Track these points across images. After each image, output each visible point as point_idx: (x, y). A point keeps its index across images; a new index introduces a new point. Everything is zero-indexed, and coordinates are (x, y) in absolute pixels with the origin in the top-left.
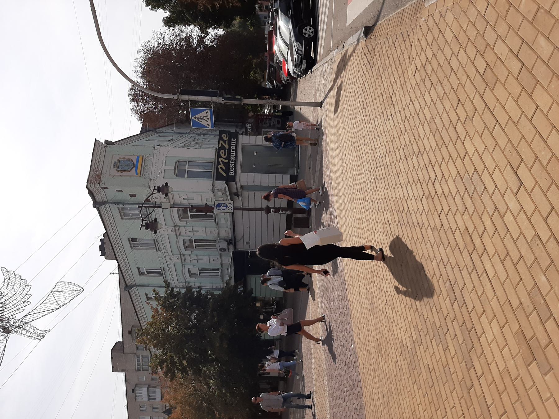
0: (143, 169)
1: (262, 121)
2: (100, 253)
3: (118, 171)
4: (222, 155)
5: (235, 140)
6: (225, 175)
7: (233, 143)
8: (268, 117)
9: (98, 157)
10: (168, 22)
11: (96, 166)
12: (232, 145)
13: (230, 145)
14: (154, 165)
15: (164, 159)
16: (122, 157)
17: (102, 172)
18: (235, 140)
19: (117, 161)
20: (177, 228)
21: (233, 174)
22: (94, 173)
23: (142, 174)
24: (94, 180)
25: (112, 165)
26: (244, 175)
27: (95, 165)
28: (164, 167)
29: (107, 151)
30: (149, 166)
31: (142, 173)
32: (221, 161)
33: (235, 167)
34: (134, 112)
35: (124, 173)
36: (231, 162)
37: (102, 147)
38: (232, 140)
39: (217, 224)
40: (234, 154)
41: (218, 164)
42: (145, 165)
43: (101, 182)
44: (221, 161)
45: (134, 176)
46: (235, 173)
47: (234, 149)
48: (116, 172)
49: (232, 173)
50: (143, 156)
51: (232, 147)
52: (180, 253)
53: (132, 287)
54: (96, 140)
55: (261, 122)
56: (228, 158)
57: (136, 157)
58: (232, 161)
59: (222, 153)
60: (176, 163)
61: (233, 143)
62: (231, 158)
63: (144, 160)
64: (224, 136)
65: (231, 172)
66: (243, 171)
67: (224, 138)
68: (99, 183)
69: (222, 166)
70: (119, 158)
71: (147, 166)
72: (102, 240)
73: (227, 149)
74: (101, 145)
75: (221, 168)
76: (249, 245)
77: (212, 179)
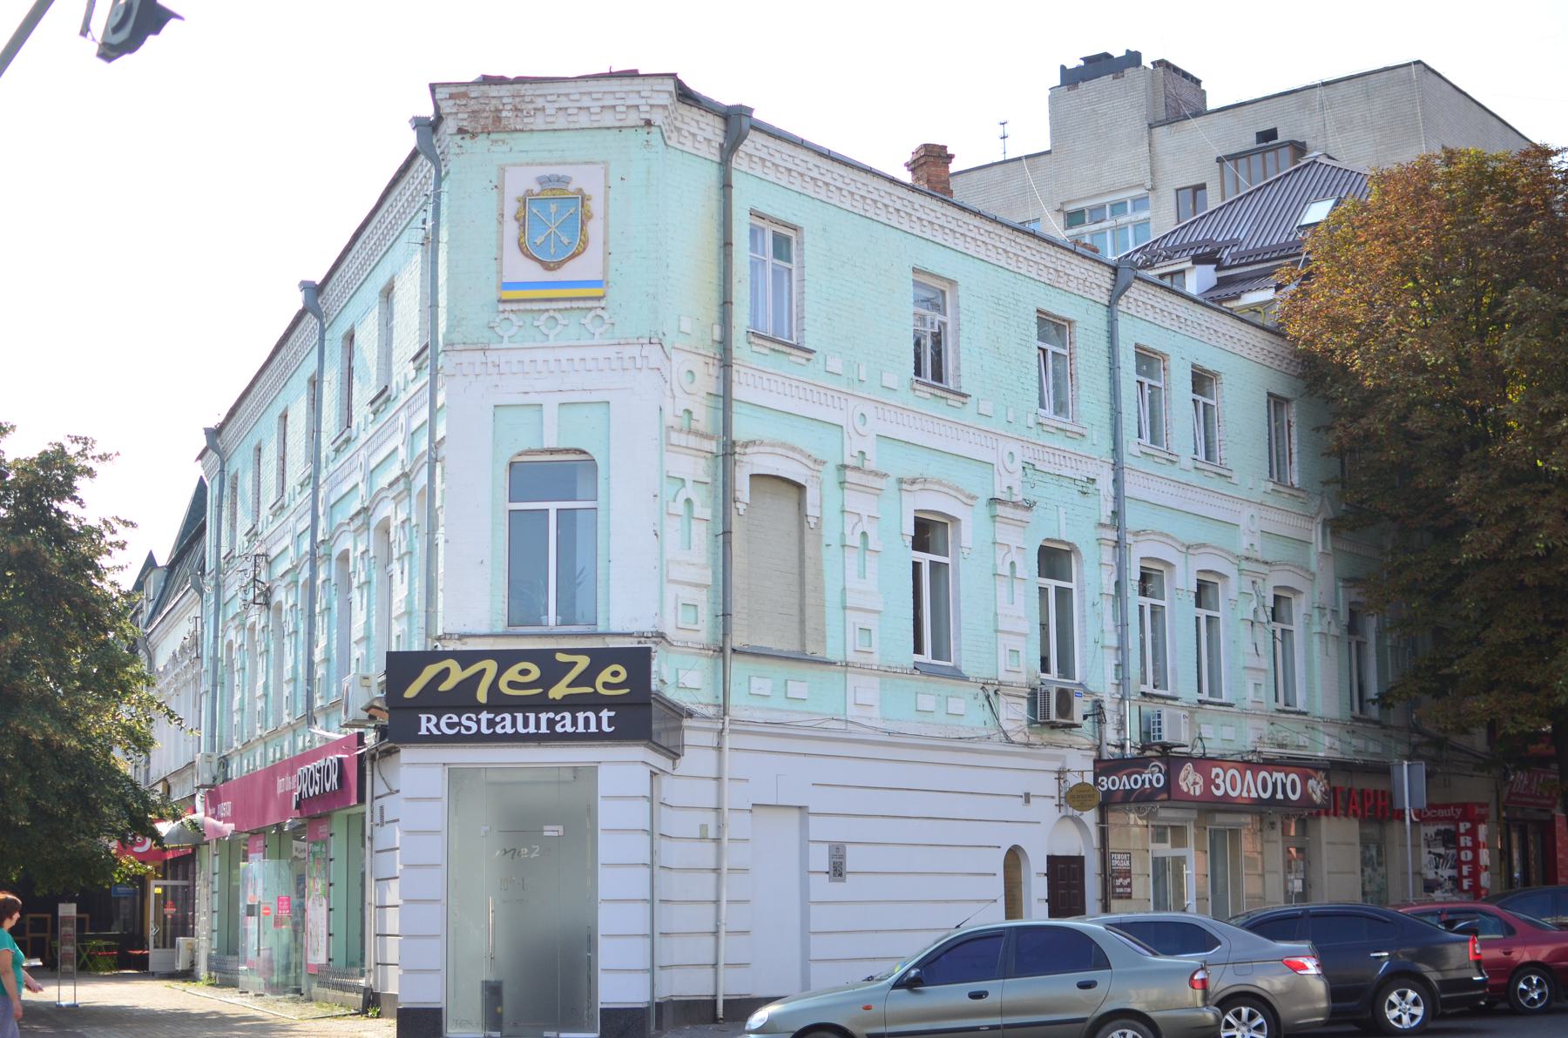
0: (535, 306)
1: (1450, 839)
2: (1074, 62)
3: (523, 201)
4: (512, 674)
6: (412, 692)
7: (587, 720)
8: (1465, 870)
9: (586, 102)
11: (540, 102)
13: (572, 704)
14: (564, 354)
16: (596, 206)
17: (516, 135)
19: (572, 188)
20: (401, 485)
21: (423, 732)
23: (508, 307)
24: (474, 105)
27: (545, 96)
28: (551, 403)
30: (552, 334)
31: (515, 307)
32: (483, 671)
33: (458, 739)
35: (512, 228)
36: (484, 716)
37: (642, 109)
38: (605, 714)
40: (532, 729)
41: (466, 658)
42: (558, 315)
43: (467, 136)
44: (483, 671)
45: (500, 272)
46: (431, 739)
47: (558, 729)
48: (521, 194)
49: (431, 726)
51: (568, 715)
53: (319, 315)
56: (498, 703)
58: (491, 724)
59: (524, 672)
60: (585, 453)
61: (587, 720)
62: (508, 716)
63: (582, 304)
64: (615, 674)
65: (434, 719)
66: (456, 775)
67: (605, 676)
68: (461, 131)
69: (457, 675)
70: (587, 192)
72: (1133, 58)
75: (445, 674)
77: (500, 629)
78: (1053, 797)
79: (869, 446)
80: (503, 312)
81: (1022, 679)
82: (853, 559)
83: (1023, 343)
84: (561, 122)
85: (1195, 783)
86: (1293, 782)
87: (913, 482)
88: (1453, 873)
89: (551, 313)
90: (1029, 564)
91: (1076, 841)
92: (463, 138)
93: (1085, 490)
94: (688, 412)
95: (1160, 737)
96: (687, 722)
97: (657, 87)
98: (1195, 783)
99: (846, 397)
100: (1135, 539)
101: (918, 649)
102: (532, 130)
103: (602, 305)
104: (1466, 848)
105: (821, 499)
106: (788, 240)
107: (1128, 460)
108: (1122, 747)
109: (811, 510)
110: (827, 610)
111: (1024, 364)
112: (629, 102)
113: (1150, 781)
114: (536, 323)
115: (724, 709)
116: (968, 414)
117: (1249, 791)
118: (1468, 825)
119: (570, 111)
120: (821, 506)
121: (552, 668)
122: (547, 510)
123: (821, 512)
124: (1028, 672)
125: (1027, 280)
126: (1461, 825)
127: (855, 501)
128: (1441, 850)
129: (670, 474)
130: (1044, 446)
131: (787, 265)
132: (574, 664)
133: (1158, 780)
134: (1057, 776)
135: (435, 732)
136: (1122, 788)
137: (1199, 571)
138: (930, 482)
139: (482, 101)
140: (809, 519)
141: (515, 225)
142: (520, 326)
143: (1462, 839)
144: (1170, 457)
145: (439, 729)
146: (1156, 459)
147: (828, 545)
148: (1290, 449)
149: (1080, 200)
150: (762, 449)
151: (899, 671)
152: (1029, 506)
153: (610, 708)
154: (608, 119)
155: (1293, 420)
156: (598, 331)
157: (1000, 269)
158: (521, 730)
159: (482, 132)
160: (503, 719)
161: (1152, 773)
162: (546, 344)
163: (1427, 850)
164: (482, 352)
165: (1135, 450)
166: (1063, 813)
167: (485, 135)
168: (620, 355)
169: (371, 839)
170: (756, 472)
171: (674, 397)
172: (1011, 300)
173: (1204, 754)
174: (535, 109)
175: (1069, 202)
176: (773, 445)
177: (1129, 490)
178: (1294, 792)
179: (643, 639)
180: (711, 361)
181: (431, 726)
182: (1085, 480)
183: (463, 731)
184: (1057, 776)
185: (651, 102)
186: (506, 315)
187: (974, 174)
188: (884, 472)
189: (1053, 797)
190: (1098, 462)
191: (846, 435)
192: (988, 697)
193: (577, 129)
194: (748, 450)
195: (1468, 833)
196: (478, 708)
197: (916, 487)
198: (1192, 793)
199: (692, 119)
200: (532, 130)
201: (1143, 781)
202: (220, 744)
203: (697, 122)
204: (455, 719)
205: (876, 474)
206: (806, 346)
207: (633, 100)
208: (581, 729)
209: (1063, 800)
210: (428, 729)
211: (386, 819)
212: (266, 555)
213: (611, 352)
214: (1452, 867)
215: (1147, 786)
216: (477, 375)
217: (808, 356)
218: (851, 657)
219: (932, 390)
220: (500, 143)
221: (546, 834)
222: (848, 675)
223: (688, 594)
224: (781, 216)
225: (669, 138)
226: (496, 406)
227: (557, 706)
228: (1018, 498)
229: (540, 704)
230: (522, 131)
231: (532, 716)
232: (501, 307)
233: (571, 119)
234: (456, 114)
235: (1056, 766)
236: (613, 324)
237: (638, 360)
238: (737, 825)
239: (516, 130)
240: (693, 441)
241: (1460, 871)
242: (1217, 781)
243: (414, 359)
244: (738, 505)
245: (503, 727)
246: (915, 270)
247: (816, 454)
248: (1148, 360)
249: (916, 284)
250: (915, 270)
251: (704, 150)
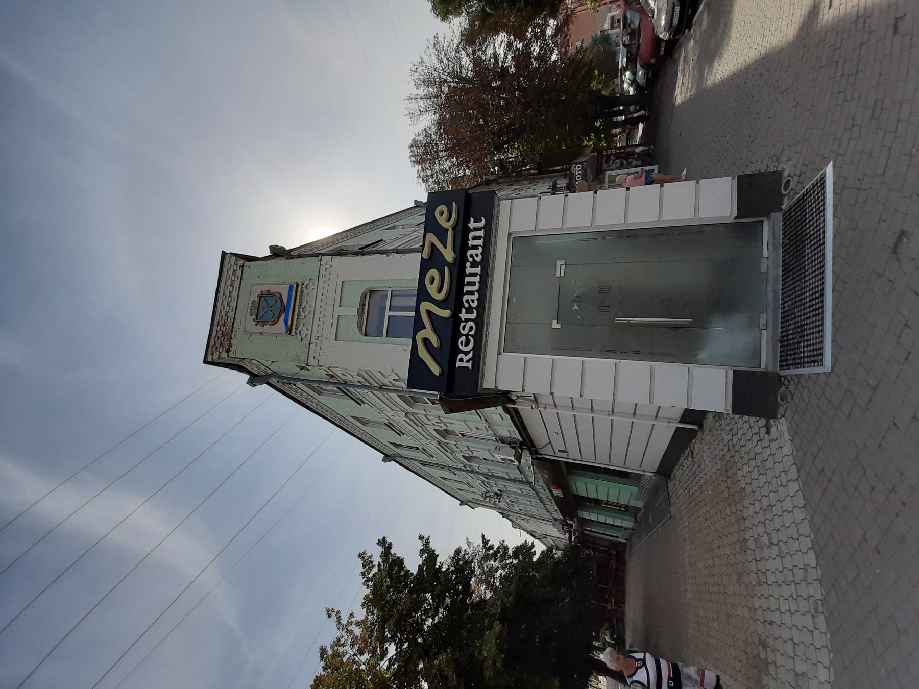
0: (296, 317)
1: (608, 160)
4: (432, 290)
5: (482, 224)
6: (436, 370)
7: (475, 238)
9: (227, 293)
10: (470, 38)
11: (223, 313)
13: (462, 247)
14: (319, 303)
15: (339, 288)
16: (265, 288)
17: (235, 326)
18: (482, 224)
19: (257, 300)
21: (469, 365)
22: (218, 329)
23: (294, 330)
24: (218, 344)
25: (249, 311)
26: (512, 360)
28: (339, 311)
29: (243, 277)
32: (429, 313)
34: (421, 180)
35: (267, 328)
36: (463, 316)
37: (235, 269)
38: (472, 224)
39: (486, 421)
42: (302, 307)
43: (231, 348)
44: (429, 313)
47: (478, 259)
49: (465, 358)
50: (298, 285)
52: (438, 441)
54: (224, 254)
55: (606, 163)
57: (288, 286)
58: (469, 311)
61: (475, 238)
62: (465, 297)
63: (299, 294)
64: (442, 214)
65: (461, 356)
66: (509, 345)
67: (442, 221)
69: (428, 332)
71: (305, 309)
75: (426, 341)
76: (566, 454)
80: (296, 333)
84: (233, 305)
89: (301, 309)
92: (231, 351)
95: (565, 187)
97: (228, 262)
102: (234, 319)
103: (300, 284)
104: (611, 152)
112: (231, 274)
113: (579, 171)
114: (303, 317)
119: (229, 300)
121: (432, 261)
122: (389, 316)
126: (604, 154)
128: (611, 161)
133: (579, 167)
135: (470, 355)
139: (217, 339)
141: (265, 326)
142: (304, 325)
145: (469, 352)
154: (237, 284)
156: (311, 287)
158: (476, 288)
159: (230, 342)
160: (467, 301)
161: (576, 170)
162: (312, 312)
164: (311, 345)
167: (232, 340)
168: (324, 276)
169: (575, 460)
174: (225, 316)
181: (465, 358)
183: (472, 333)
185: (233, 265)
186: (298, 332)
193: (238, 298)
195: (606, 152)
196: (456, 320)
200: (234, 319)
201: (579, 174)
202: (550, 519)
204: (463, 339)
207: (231, 272)
208: (481, 242)
210: (468, 361)
211: (565, 450)
212: (486, 492)
215: (580, 172)
216: (320, 349)
221: (562, 275)
226: (336, 340)
227: (461, 259)
230: (233, 323)
231: (467, 279)
232: (293, 334)
233: (233, 300)
234: (220, 352)
236: (310, 279)
237: (327, 267)
239: (233, 326)
243: (360, 405)
245: (473, 301)
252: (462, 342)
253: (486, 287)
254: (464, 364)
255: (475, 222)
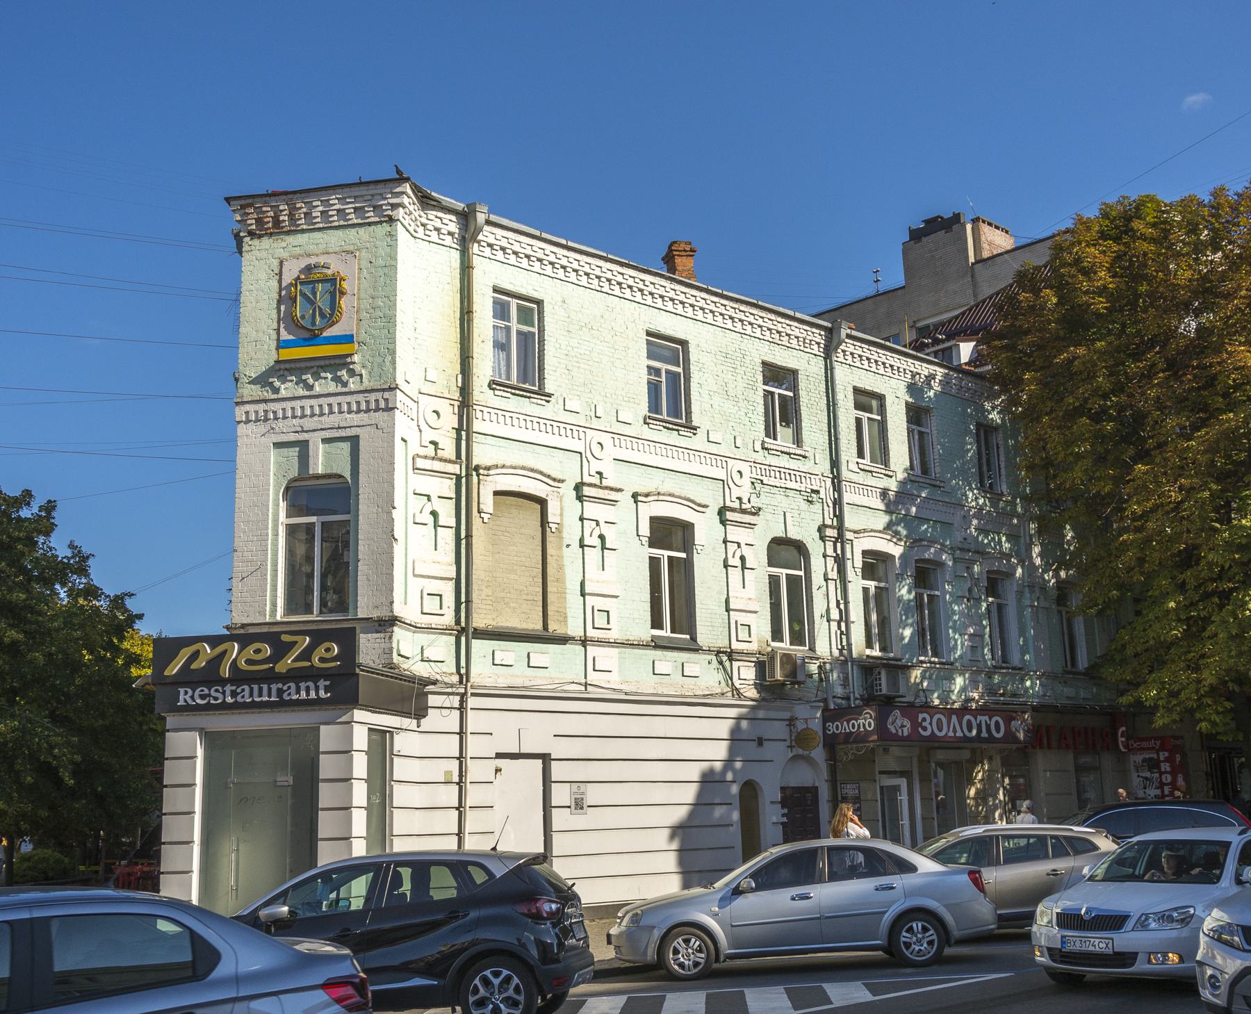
1: (1153, 765)
5: (322, 694)
8: (1167, 790)
12: (303, 685)
13: (296, 676)
18: (322, 694)
21: (181, 703)
23: (283, 366)
28: (315, 440)
31: (287, 366)
32: (225, 652)
33: (208, 708)
36: (229, 688)
41: (214, 641)
44: (225, 652)
46: (188, 708)
47: (286, 697)
49: (187, 698)
59: (258, 651)
62: (246, 688)
67: (320, 651)
73: (273, 667)
74: (391, 201)
75: (195, 655)
78: (785, 740)
79: (608, 468)
80: (280, 369)
81: (753, 647)
82: (593, 555)
83: (750, 387)
85: (903, 726)
86: (997, 723)
87: (647, 495)
88: (1158, 792)
90: (758, 557)
91: (813, 775)
93: (810, 499)
94: (434, 443)
95: (881, 690)
96: (430, 688)
98: (903, 726)
99: (584, 429)
100: (856, 535)
101: (656, 623)
104: (1166, 772)
105: (562, 509)
106: (532, 310)
107: (845, 474)
108: (848, 699)
109: (552, 517)
110: (568, 596)
111: (751, 403)
115: (464, 678)
116: (698, 442)
117: (955, 731)
118: (1167, 754)
120: (561, 515)
123: (562, 520)
124: (759, 641)
125: (753, 339)
126: (1161, 754)
127: (591, 510)
128: (1148, 774)
129: (416, 492)
130: (770, 466)
131: (531, 329)
132: (296, 643)
133: (870, 725)
134: (787, 723)
136: (843, 731)
137: (917, 561)
138: (664, 495)
140: (551, 525)
143: (1162, 764)
144: (887, 472)
146: (874, 474)
147: (568, 546)
148: (999, 465)
149: (925, 318)
150: (504, 471)
151: (635, 643)
152: (756, 512)
153: (326, 678)
155: (1000, 443)
157: (727, 331)
158: (257, 699)
160: (243, 690)
161: (865, 719)
163: (1137, 774)
165: (853, 467)
166: (794, 753)
170: (499, 488)
171: (420, 431)
172: (737, 354)
173: (926, 703)
175: (919, 320)
176: (515, 468)
177: (847, 497)
178: (998, 730)
179: (382, 623)
180: (452, 402)
181: (187, 698)
182: (809, 491)
183: (212, 702)
184: (787, 723)
186: (281, 372)
187: (855, 306)
188: (619, 487)
189: (785, 740)
190: (822, 478)
191: (584, 459)
192: (721, 663)
194: (491, 472)
195: (1166, 760)
196: (223, 682)
197: (650, 499)
198: (900, 734)
199: (436, 217)
201: (859, 725)
203: (441, 219)
204: (206, 691)
205: (612, 489)
206: (546, 391)
209: (794, 743)
210: (185, 701)
213: (360, 397)
214: (1157, 788)
215: (862, 729)
217: (547, 399)
218: (591, 633)
219: (664, 424)
220: (280, 241)
221: (278, 784)
222: (588, 647)
223: (436, 586)
224: (523, 291)
225: (415, 231)
228: (744, 506)
229: (270, 677)
231: (265, 687)
235: (787, 715)
238: (476, 771)
240: (437, 466)
241: (1163, 791)
242: (924, 724)
244: (482, 515)
245: (243, 697)
246: (649, 334)
247: (554, 476)
248: (866, 399)
249: (648, 342)
250: (649, 334)
251: (448, 240)
252: (202, 691)
253: (260, 708)
254: (182, 697)
255: (325, 686)
